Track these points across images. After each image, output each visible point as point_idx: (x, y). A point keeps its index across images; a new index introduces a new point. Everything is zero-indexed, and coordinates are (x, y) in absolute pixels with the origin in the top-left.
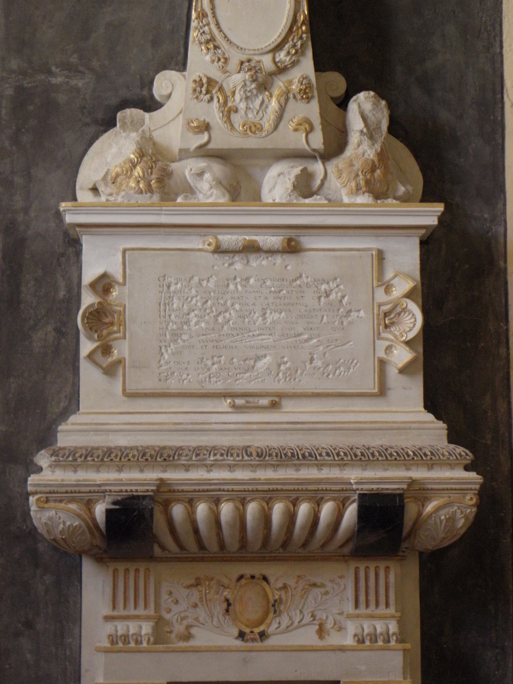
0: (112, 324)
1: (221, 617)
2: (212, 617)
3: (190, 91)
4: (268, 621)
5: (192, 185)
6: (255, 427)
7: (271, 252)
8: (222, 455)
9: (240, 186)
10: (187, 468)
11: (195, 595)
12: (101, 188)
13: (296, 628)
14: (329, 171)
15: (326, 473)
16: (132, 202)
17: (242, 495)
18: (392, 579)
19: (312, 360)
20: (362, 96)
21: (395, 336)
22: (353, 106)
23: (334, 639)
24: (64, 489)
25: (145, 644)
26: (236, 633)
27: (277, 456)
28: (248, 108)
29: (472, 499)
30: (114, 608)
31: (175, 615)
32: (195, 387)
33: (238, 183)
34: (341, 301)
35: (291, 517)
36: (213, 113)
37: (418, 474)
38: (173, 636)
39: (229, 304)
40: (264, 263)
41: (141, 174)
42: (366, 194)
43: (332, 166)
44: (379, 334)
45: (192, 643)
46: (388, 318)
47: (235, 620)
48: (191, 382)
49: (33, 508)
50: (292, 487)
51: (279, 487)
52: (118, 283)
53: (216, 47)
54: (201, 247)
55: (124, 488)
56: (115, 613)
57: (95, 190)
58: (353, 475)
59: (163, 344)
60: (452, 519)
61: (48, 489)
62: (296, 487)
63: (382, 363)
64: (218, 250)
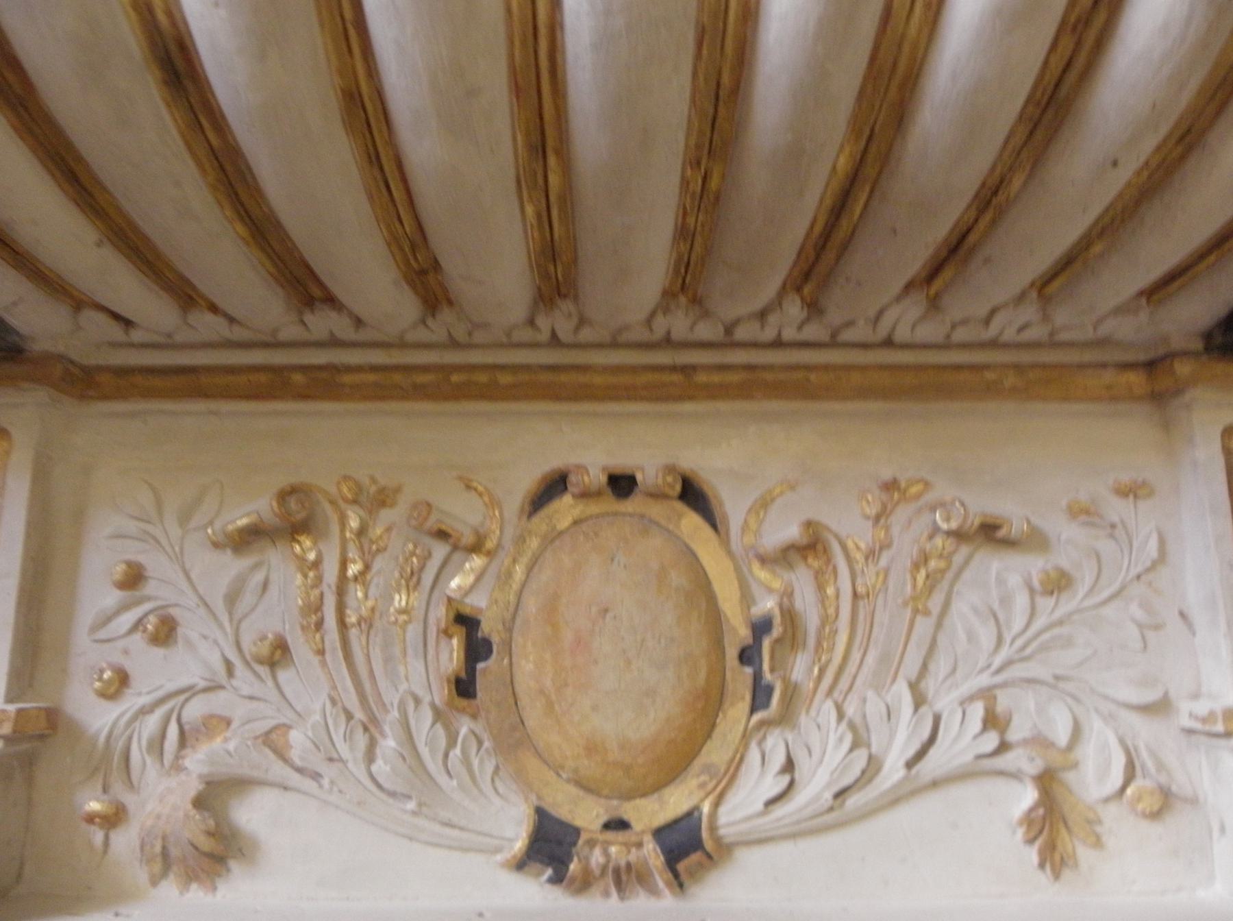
1: (423, 723)
2: (372, 726)
4: (716, 753)
13: (894, 799)
26: (516, 833)
31: (145, 711)
38: (125, 841)
47: (513, 741)
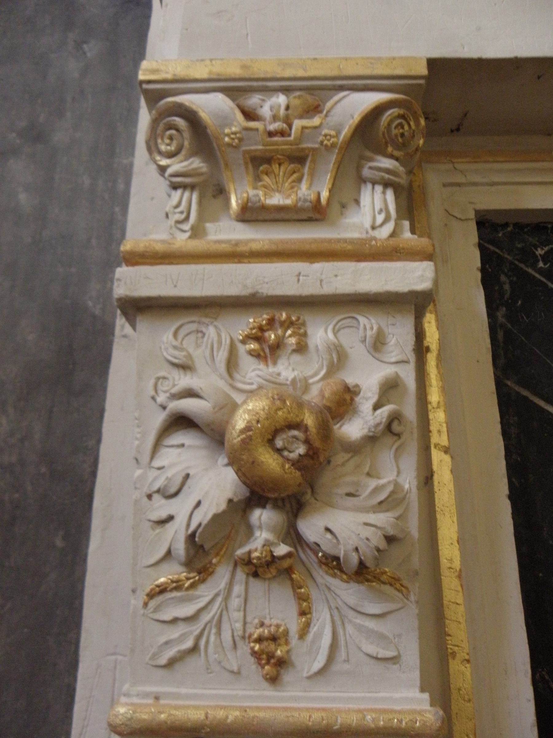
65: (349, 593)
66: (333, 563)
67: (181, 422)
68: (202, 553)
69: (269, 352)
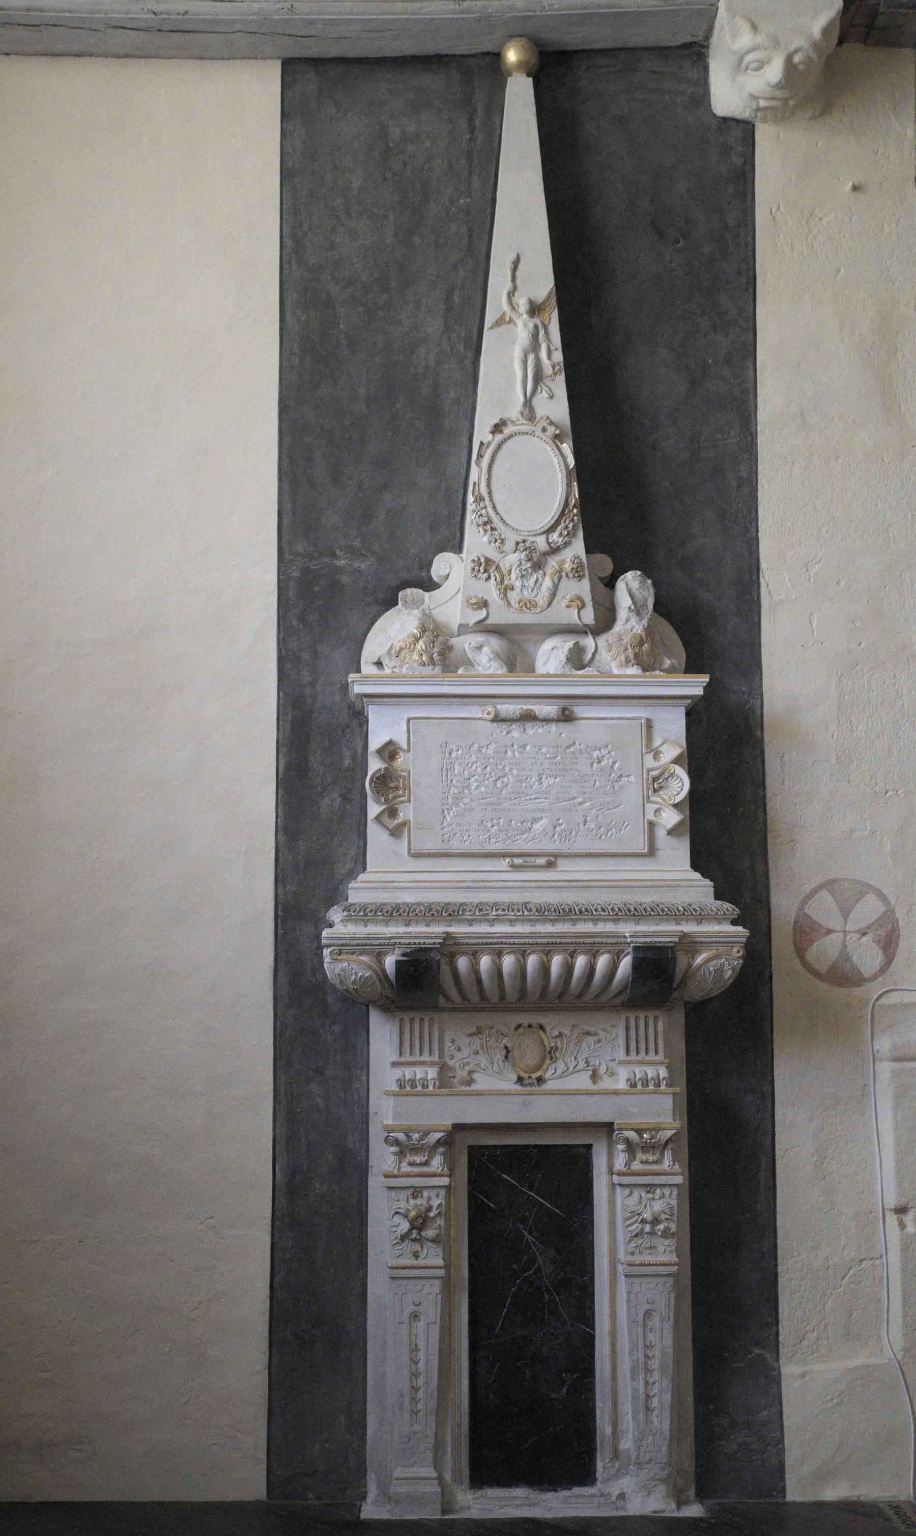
0: (397, 788)
2: (492, 1063)
3: (469, 570)
4: (545, 1067)
5: (471, 658)
6: (533, 884)
7: (546, 720)
8: (503, 910)
9: (516, 660)
10: (470, 923)
11: (477, 1042)
12: (385, 662)
13: (571, 1074)
14: (599, 645)
15: (601, 927)
16: (417, 673)
17: (523, 947)
18: (660, 1027)
19: (585, 822)
20: (629, 575)
21: (664, 800)
22: (621, 585)
23: (606, 1083)
24: (356, 942)
25: (431, 1088)
27: (555, 911)
28: (523, 586)
29: (739, 951)
30: (401, 1054)
32: (476, 848)
33: (514, 656)
34: (612, 766)
35: (568, 969)
36: (491, 591)
37: (689, 928)
38: (456, 1081)
39: (507, 769)
40: (540, 730)
41: (424, 647)
42: (635, 667)
43: (602, 640)
44: (649, 798)
45: (474, 1087)
46: (656, 783)
47: (514, 1066)
48: (472, 843)
49: (327, 960)
50: (569, 940)
51: (558, 940)
52: (403, 750)
53: (493, 529)
54: (480, 716)
55: (412, 941)
56: (402, 1060)
57: (379, 664)
58: (627, 929)
59: (445, 807)
60: (720, 971)
61: (340, 942)
62: (574, 940)
63: (652, 825)
64: (497, 719)
65: (430, 1244)
66: (427, 1239)
67: (397, 1213)
68: (403, 1238)
69: (415, 1197)
